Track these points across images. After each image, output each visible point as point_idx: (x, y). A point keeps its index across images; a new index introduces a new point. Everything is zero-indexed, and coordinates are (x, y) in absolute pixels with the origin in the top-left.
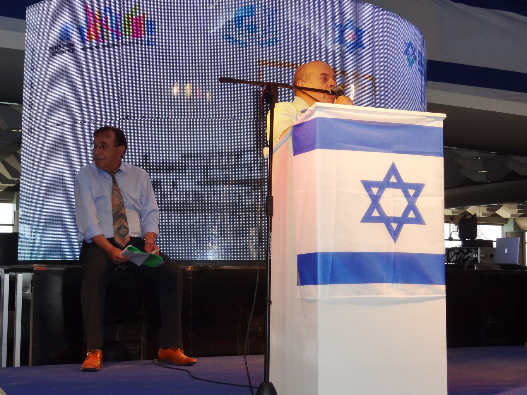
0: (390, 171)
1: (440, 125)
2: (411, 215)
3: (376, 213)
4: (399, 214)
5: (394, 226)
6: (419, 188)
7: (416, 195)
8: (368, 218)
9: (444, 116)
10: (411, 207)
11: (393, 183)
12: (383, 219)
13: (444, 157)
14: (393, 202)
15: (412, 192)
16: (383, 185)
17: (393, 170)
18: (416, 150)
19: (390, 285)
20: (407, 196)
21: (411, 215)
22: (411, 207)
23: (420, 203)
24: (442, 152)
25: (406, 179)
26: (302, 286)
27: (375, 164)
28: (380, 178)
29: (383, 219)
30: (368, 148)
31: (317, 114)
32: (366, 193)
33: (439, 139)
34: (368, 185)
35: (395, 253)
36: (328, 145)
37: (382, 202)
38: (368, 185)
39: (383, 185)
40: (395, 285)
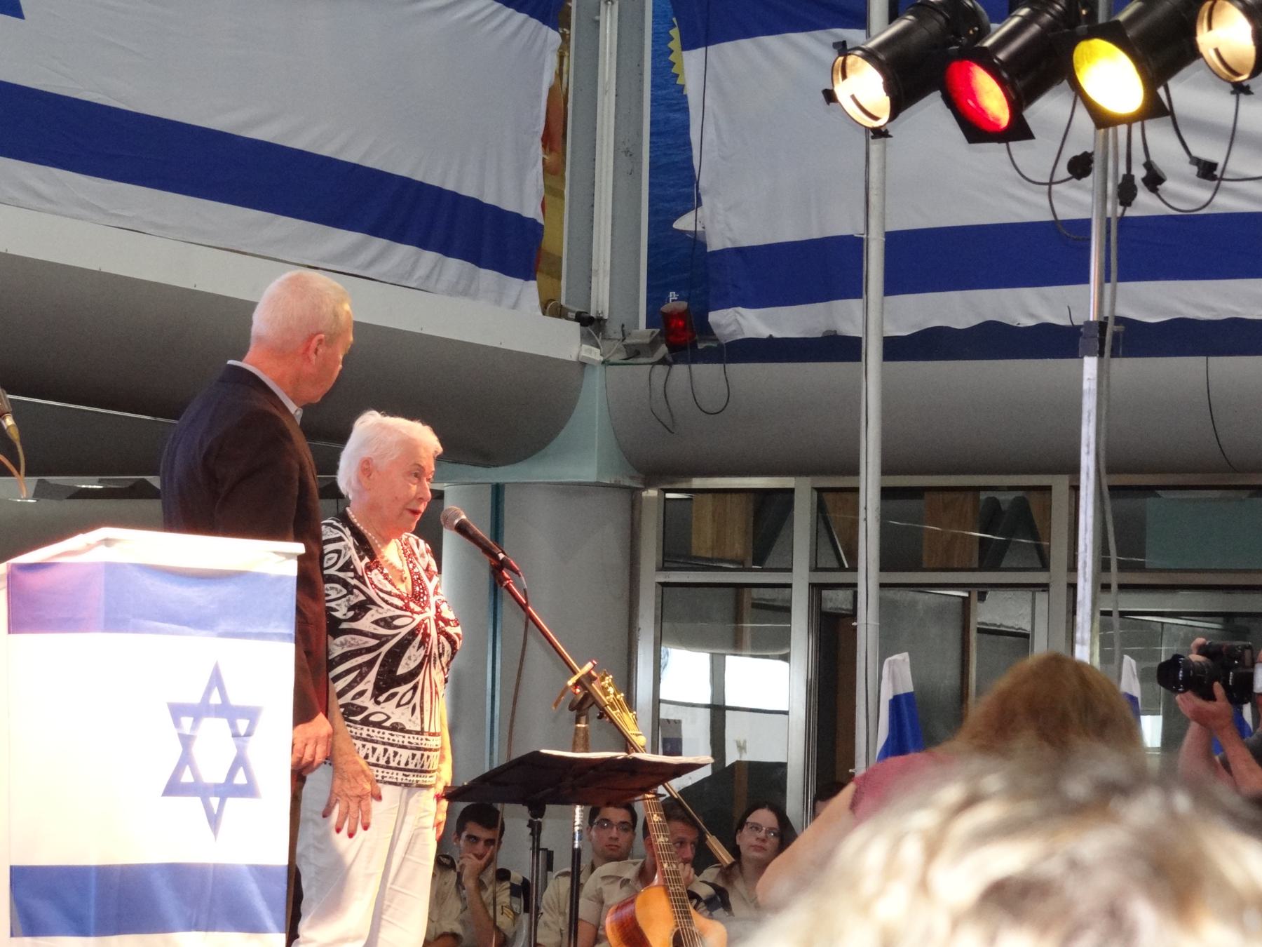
0: (211, 678)
1: (292, 569)
2: (240, 779)
3: (187, 777)
4: (221, 779)
5: (215, 801)
6: (252, 714)
7: (248, 734)
8: (174, 788)
9: (300, 548)
10: (240, 761)
11: (216, 706)
12: (198, 789)
13: (297, 643)
14: (214, 753)
15: (242, 725)
16: (198, 712)
17: (216, 680)
18: (255, 630)
19: (202, 933)
20: (236, 735)
21: (240, 779)
22: (240, 761)
23: (253, 749)
25: (235, 700)
26: (28, 940)
27: (176, 661)
28: (195, 698)
29: (198, 789)
31: (102, 555)
32: (174, 732)
34: (177, 711)
35: (215, 866)
36: (115, 622)
37: (197, 750)
38: (177, 711)
39: (198, 712)
40: (210, 934)
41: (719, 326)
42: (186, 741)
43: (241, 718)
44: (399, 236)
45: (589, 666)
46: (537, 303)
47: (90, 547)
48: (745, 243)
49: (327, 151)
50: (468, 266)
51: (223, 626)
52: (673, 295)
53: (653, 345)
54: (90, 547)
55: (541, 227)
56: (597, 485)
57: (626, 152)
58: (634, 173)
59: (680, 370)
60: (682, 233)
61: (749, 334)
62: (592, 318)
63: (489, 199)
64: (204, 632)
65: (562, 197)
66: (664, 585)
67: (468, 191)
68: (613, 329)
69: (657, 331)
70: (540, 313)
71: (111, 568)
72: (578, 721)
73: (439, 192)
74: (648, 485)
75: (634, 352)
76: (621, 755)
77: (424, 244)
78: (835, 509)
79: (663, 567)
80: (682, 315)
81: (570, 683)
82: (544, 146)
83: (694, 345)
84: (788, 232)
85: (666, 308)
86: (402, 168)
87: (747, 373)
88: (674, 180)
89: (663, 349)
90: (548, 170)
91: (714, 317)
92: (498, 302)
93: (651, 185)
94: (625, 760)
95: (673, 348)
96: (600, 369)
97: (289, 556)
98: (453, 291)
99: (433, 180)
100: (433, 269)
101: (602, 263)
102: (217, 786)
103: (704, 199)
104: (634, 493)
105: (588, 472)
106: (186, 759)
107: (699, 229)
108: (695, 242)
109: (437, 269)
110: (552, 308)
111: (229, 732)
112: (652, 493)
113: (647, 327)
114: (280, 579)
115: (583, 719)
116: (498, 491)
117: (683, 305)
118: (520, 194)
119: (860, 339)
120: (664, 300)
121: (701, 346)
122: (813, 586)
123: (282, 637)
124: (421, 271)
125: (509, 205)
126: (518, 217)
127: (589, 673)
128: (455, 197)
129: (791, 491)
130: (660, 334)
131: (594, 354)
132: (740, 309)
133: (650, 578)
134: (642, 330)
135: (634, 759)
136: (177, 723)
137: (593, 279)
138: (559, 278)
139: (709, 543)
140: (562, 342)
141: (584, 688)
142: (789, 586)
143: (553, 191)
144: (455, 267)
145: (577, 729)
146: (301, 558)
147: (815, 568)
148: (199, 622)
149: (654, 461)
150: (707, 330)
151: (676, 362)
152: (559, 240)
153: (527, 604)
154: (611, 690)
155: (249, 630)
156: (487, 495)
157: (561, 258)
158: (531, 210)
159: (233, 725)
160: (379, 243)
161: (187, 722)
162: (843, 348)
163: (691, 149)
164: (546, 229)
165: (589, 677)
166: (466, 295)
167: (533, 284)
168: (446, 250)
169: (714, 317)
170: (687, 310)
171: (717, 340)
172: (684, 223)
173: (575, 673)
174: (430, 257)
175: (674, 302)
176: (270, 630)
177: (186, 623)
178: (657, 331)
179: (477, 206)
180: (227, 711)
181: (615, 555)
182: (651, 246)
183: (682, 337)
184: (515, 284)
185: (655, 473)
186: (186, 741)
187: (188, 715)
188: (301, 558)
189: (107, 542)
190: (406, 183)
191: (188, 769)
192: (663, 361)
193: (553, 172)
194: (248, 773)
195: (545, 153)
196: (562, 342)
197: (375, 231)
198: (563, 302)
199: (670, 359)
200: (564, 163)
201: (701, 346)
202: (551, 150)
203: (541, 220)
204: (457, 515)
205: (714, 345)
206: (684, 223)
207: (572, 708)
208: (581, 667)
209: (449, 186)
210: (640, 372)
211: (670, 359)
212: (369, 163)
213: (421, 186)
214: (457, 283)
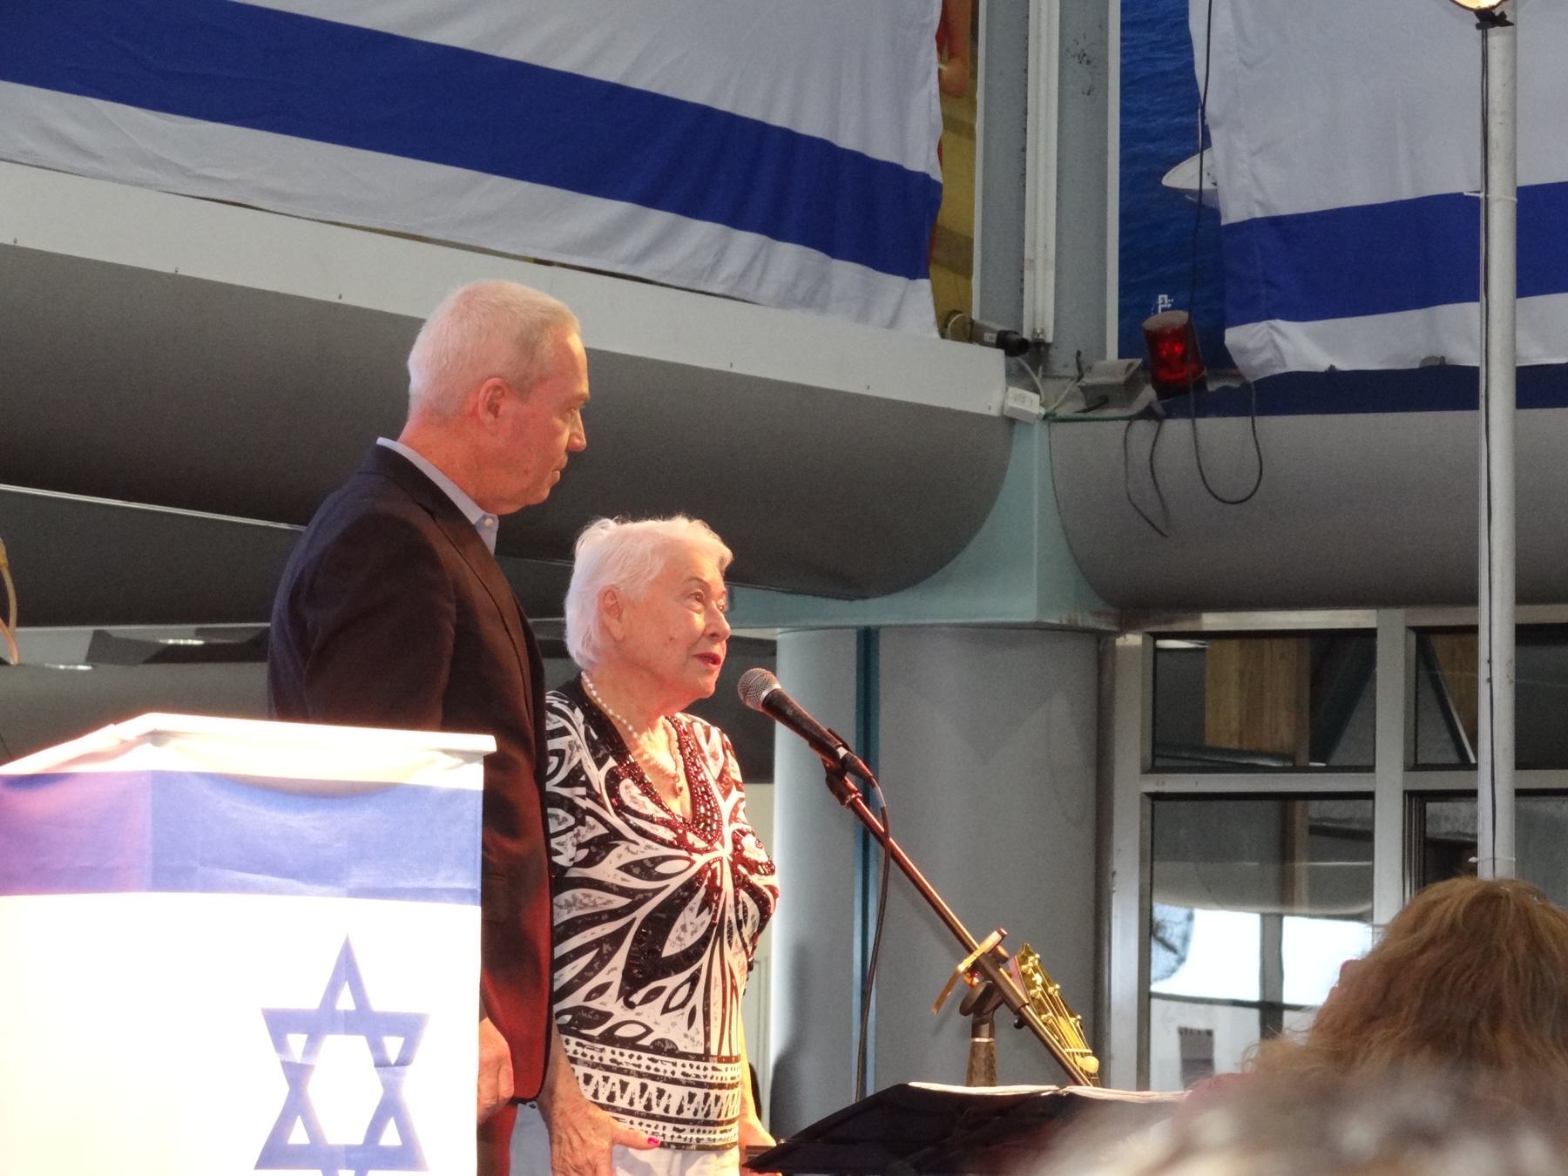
0: (338, 966)
1: (473, 779)
3: (298, 1136)
4: (357, 1138)
6: (409, 1027)
7: (403, 1062)
9: (487, 743)
10: (389, 1108)
11: (346, 1013)
16: (317, 1024)
17: (347, 969)
20: (381, 1064)
21: (390, 1137)
23: (414, 1088)
24: (476, 885)
27: (280, 938)
28: (310, 1000)
30: (275, 880)
32: (275, 1060)
33: (469, 831)
34: (279, 1024)
36: (173, 871)
37: (315, 1089)
38: (279, 1024)
39: (317, 1024)
41: (1243, 351)
42: (296, 1075)
43: (391, 1035)
44: (692, 208)
45: (994, 938)
46: (931, 317)
47: (126, 747)
48: (1286, 208)
49: (565, 63)
50: (815, 256)
51: (358, 878)
52: (1163, 300)
53: (1130, 387)
54: (126, 747)
55: (938, 187)
56: (1039, 627)
57: (1079, 57)
58: (1095, 91)
59: (1177, 429)
60: (1177, 193)
61: (1293, 366)
62: (1024, 341)
63: (847, 140)
64: (324, 889)
65: (971, 135)
66: (1156, 797)
67: (811, 125)
68: (1062, 360)
69: (1138, 362)
70: (936, 335)
71: (163, 781)
72: (976, 1033)
73: (761, 130)
74: (1126, 626)
75: (1098, 399)
76: (1047, 1089)
77: (736, 219)
78: (1443, 660)
79: (1153, 767)
80: (1179, 335)
81: (962, 967)
82: (940, 50)
83: (1201, 385)
84: (1360, 190)
85: (1152, 323)
86: (697, 94)
87: (1291, 433)
88: (1163, 101)
89: (1148, 394)
90: (944, 89)
91: (1234, 336)
92: (863, 316)
93: (1124, 112)
94: (1055, 1097)
95: (1163, 392)
96: (1039, 430)
97: (468, 756)
98: (787, 300)
99: (750, 109)
100: (755, 258)
101: (1040, 249)
102: (350, 1149)
103: (1215, 135)
104: (1101, 642)
105: (1018, 601)
106: (296, 1105)
107: (1207, 185)
108: (1201, 208)
109: (758, 265)
110: (956, 325)
111: (368, 1058)
112: (1133, 640)
113: (1121, 355)
114: (455, 796)
115: (985, 1028)
116: (868, 639)
117: (1181, 317)
118: (903, 133)
119: (1476, 370)
120: (1149, 308)
121: (1212, 387)
122: (1410, 795)
123: (460, 896)
124: (734, 263)
125: (881, 150)
126: (896, 172)
127: (994, 950)
128: (789, 137)
129: (1369, 634)
130: (1144, 367)
131: (1029, 403)
132: (1279, 323)
133: (1132, 782)
134: (1111, 362)
135: (1072, 1096)
136: (280, 1045)
137: (1027, 274)
138: (967, 273)
139: (1234, 726)
140: (976, 383)
141: (986, 976)
142: (1370, 796)
143: (956, 126)
144: (789, 256)
145: (975, 1045)
146: (490, 761)
147: (1414, 765)
148: (316, 871)
149: (1134, 584)
150: (1222, 360)
151: (1169, 416)
152: (970, 210)
153: (886, 834)
154: (1038, 978)
155: (402, 884)
156: (850, 646)
157: (969, 242)
158: (920, 158)
159: (376, 1046)
160: (658, 220)
161: (297, 1042)
162: (1450, 387)
163: (1190, 51)
164: (946, 193)
165: (995, 958)
166: (809, 306)
167: (924, 284)
168: (775, 229)
169: (1234, 336)
170: (1187, 327)
171: (1239, 376)
172: (1182, 177)
173: (970, 950)
174: (746, 241)
175: (1166, 312)
176: (440, 883)
177: (294, 875)
178: (1138, 362)
179: (824, 151)
180: (366, 1022)
181: (1072, 751)
182: (1124, 217)
183: (1180, 371)
184: (893, 285)
185: (1138, 605)
186: (296, 1075)
187: (297, 1030)
188: (490, 761)
189: (156, 737)
190: (705, 115)
191: (299, 1122)
192: (1148, 414)
193: (956, 92)
194: (404, 1129)
195: (941, 61)
196: (976, 383)
197: (651, 198)
198: (975, 316)
199: (1158, 408)
200: (974, 75)
201: (1212, 387)
202: (952, 55)
203: (937, 176)
204: (766, 684)
205: (1235, 385)
206: (1182, 177)
207: (964, 1011)
208: (981, 940)
209: (778, 120)
210: (1108, 432)
211: (1158, 408)
212: (640, 83)
213: (731, 120)
214: (795, 285)
